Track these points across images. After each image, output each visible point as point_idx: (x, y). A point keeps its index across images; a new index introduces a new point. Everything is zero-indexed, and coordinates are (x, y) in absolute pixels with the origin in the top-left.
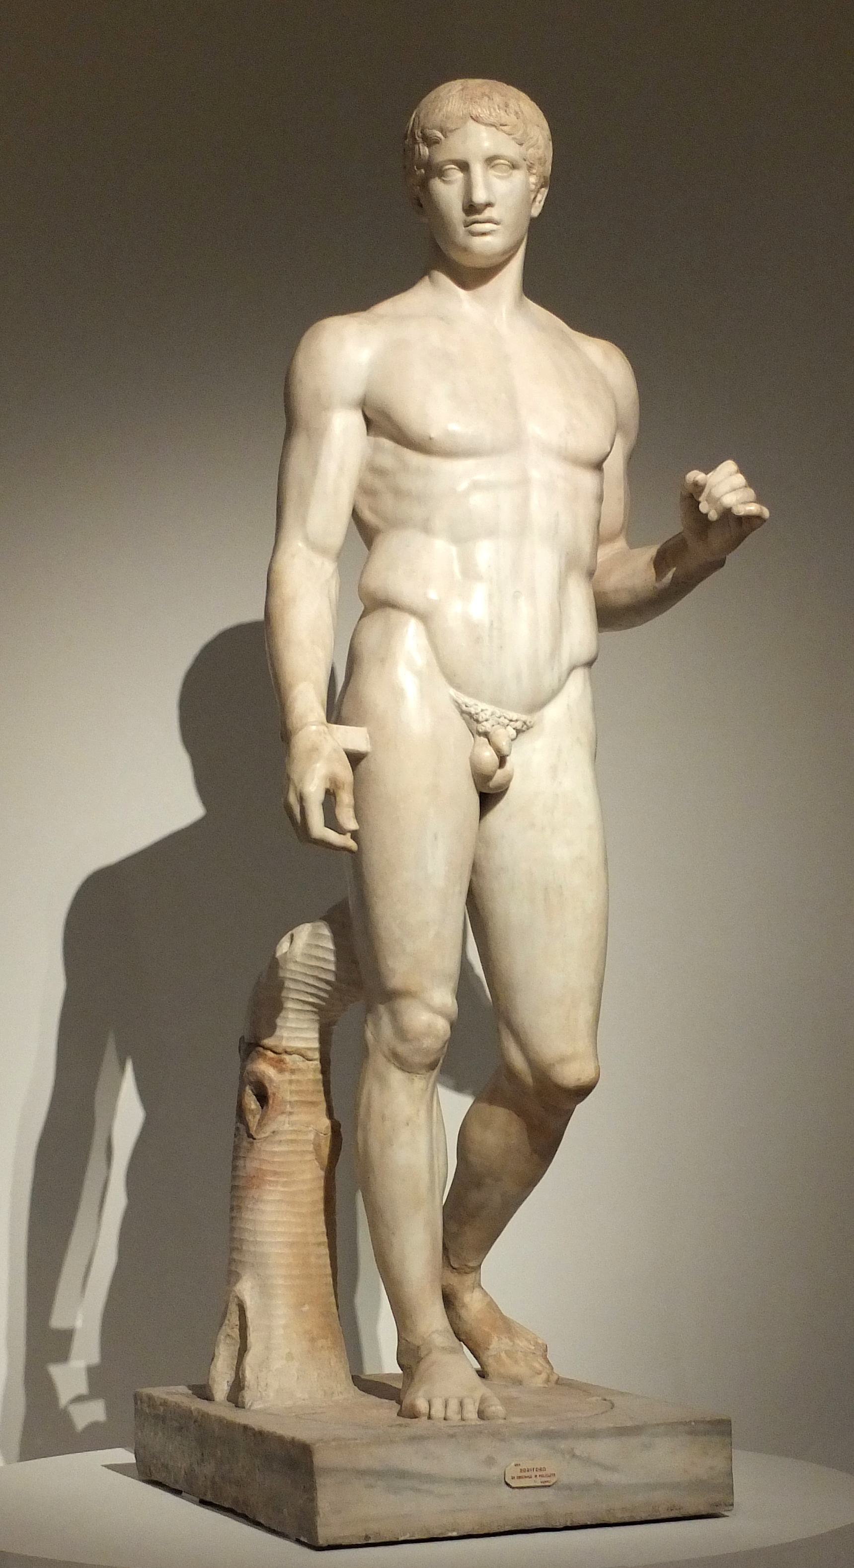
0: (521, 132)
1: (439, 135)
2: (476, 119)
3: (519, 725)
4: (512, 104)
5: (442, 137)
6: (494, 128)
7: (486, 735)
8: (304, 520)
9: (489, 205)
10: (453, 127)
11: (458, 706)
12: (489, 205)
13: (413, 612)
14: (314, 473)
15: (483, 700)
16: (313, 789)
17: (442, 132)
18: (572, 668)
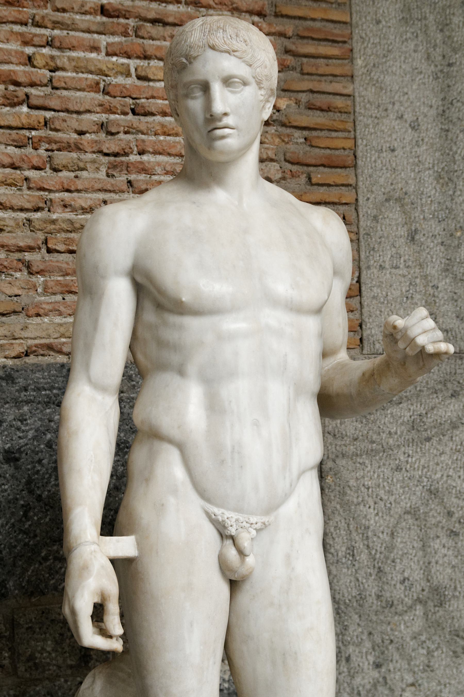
0: (250, 56)
1: (184, 60)
2: (213, 48)
3: (259, 526)
4: (243, 33)
5: (187, 63)
6: (228, 55)
7: (232, 538)
8: (87, 366)
9: (226, 114)
10: (195, 55)
11: (208, 514)
12: (226, 114)
13: (170, 441)
14: (95, 328)
15: (228, 509)
16: (82, 603)
17: (186, 59)
18: (302, 473)
